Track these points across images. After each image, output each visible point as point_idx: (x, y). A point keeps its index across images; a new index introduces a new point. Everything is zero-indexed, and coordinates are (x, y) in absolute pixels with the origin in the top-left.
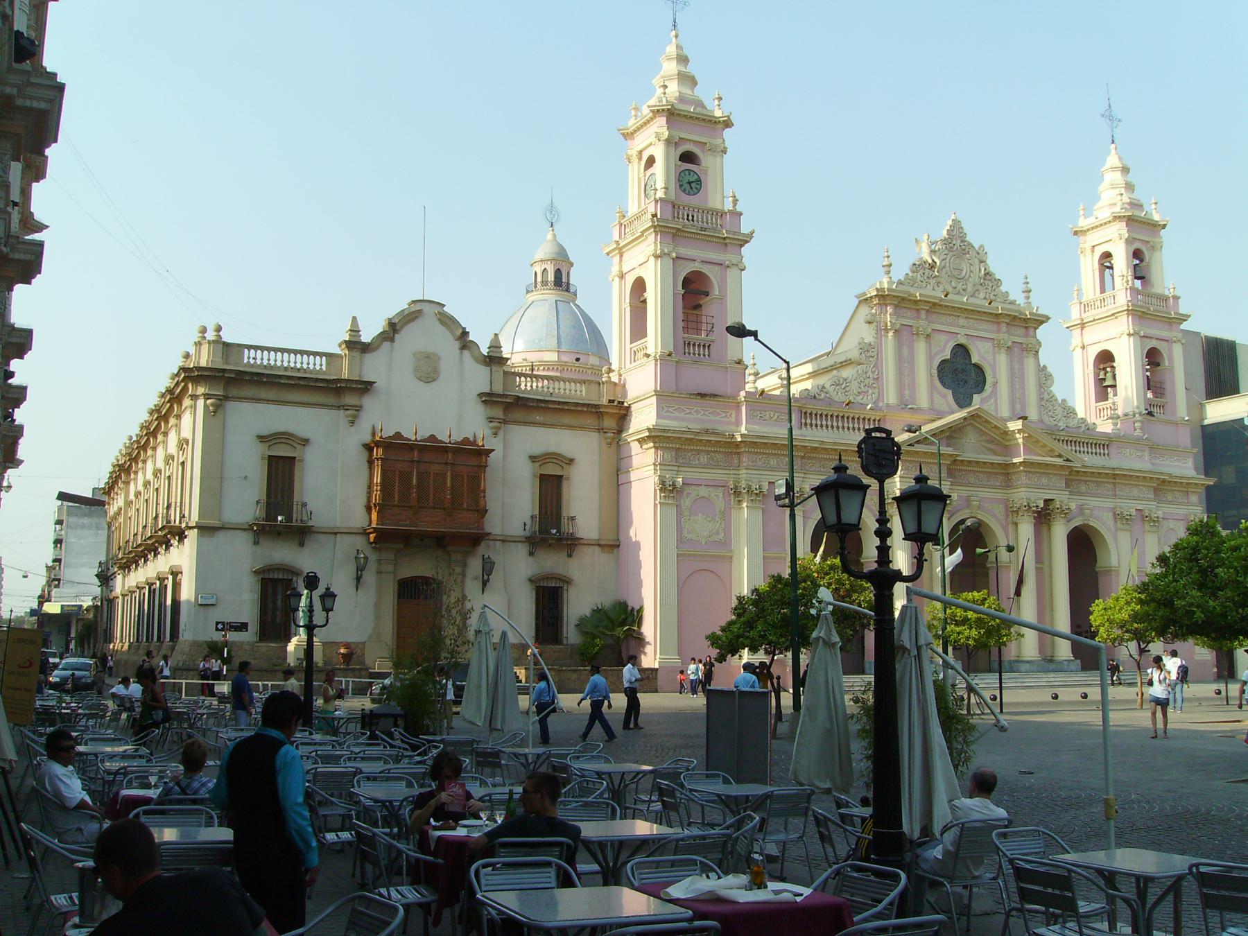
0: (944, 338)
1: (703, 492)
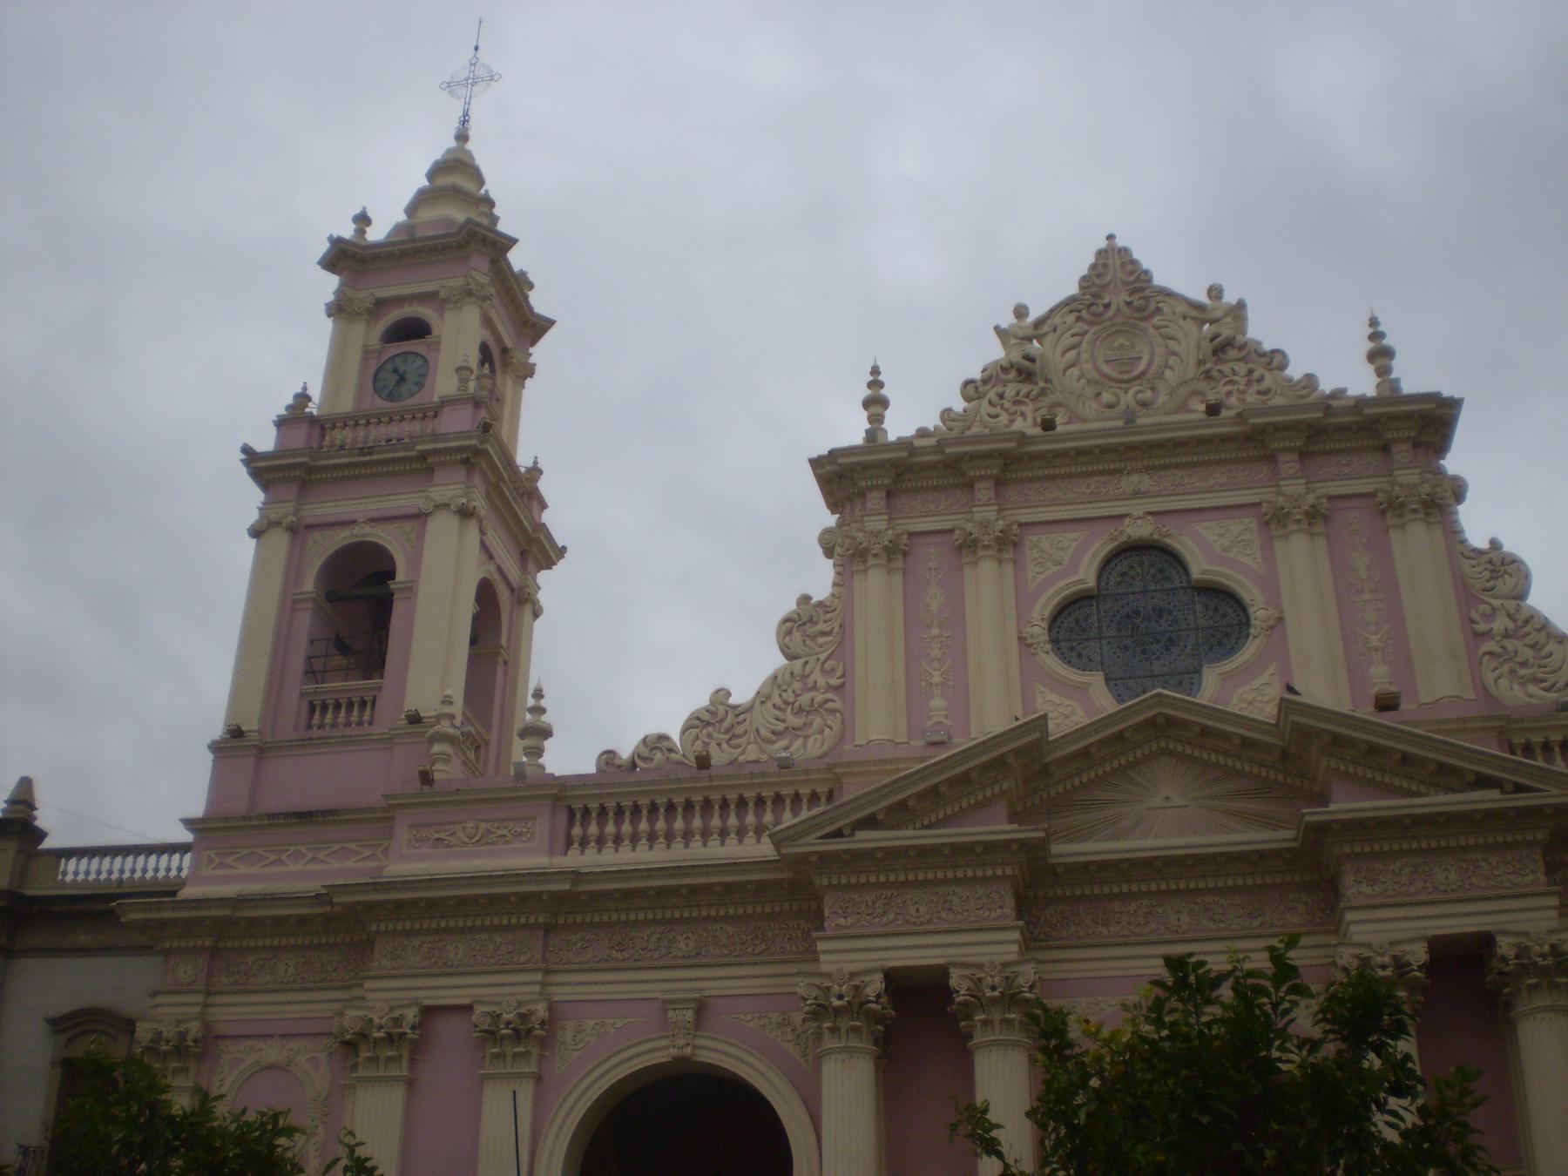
0: (1069, 540)
1: (273, 1052)
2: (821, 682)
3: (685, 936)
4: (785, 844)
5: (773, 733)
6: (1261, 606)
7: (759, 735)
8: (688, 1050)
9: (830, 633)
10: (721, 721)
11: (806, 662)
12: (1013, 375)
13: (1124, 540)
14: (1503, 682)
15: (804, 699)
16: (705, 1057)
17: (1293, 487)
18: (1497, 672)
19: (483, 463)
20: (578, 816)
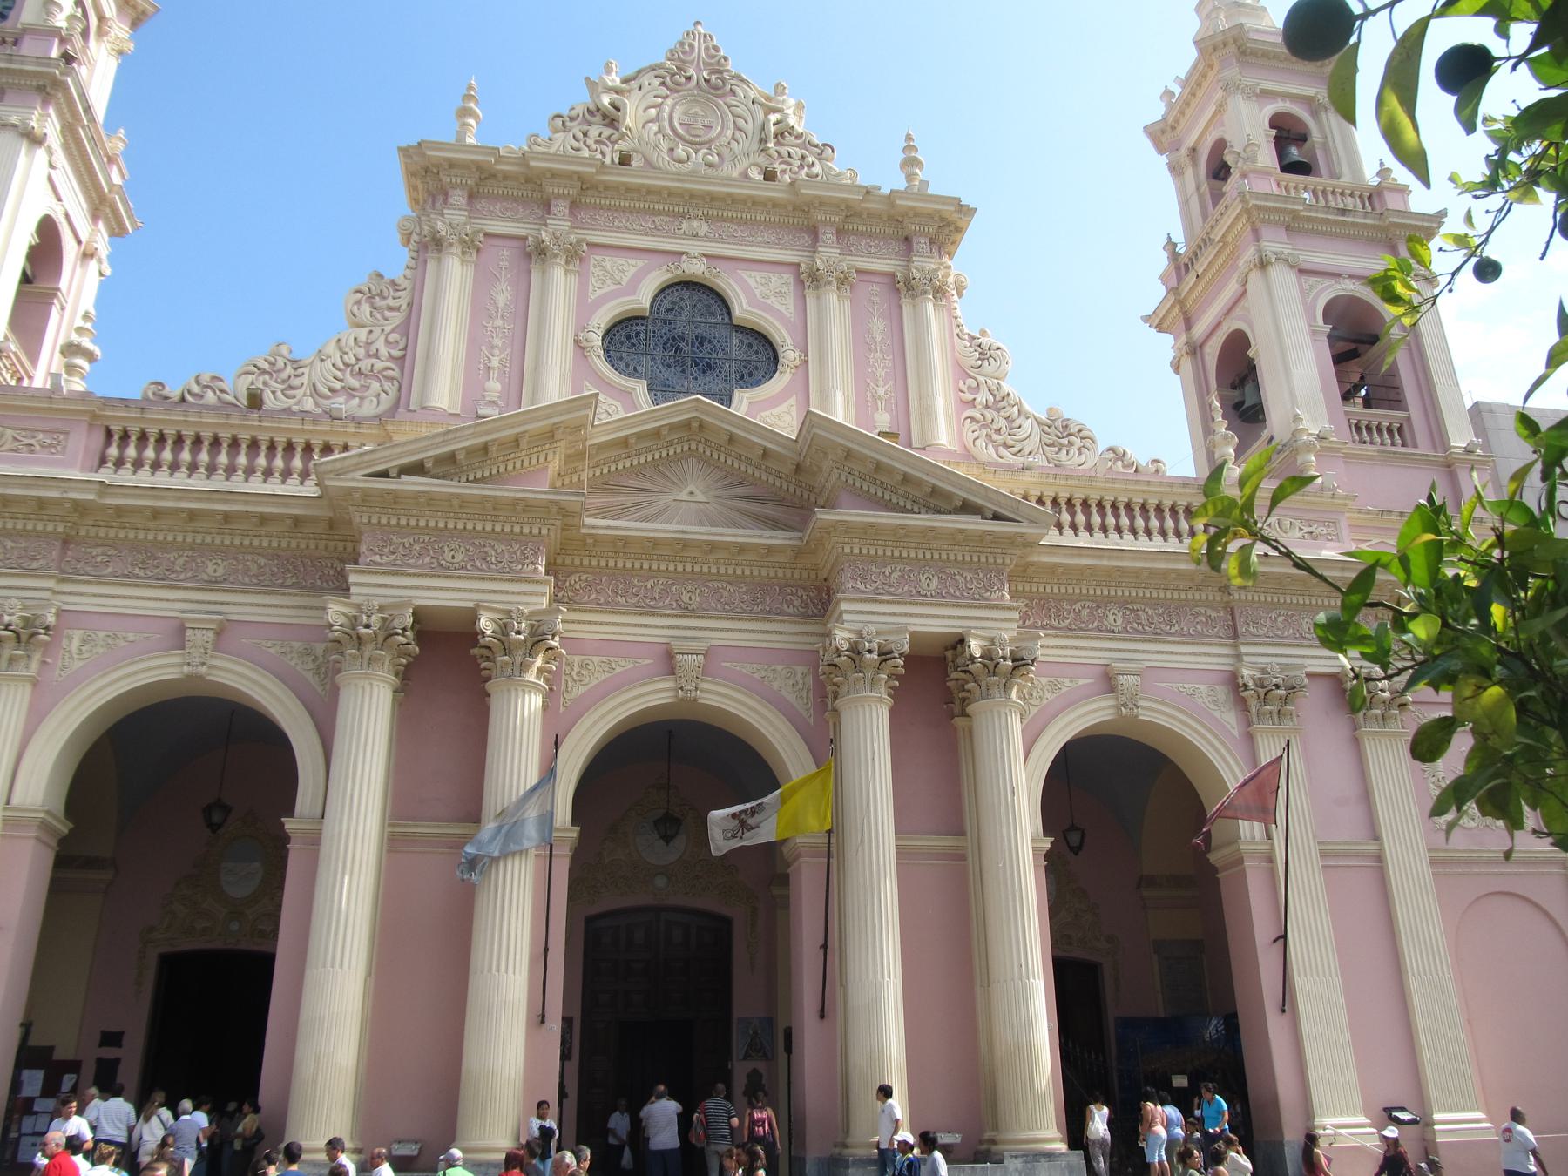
0: (632, 265)
2: (384, 351)
3: (214, 561)
4: (328, 476)
5: (331, 390)
6: (791, 347)
7: (315, 390)
8: (203, 669)
9: (398, 309)
10: (279, 371)
11: (371, 331)
12: (598, 118)
13: (679, 272)
14: (981, 442)
15: (365, 365)
16: (218, 677)
17: (828, 255)
18: (976, 434)
19: (60, 95)
20: (116, 437)
